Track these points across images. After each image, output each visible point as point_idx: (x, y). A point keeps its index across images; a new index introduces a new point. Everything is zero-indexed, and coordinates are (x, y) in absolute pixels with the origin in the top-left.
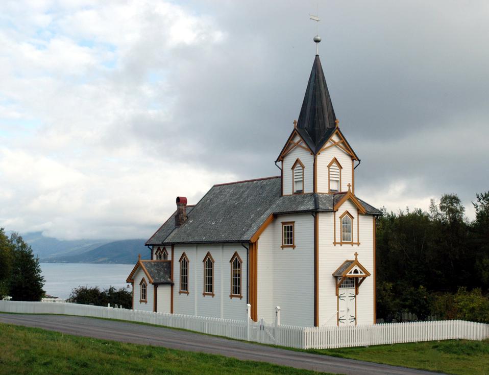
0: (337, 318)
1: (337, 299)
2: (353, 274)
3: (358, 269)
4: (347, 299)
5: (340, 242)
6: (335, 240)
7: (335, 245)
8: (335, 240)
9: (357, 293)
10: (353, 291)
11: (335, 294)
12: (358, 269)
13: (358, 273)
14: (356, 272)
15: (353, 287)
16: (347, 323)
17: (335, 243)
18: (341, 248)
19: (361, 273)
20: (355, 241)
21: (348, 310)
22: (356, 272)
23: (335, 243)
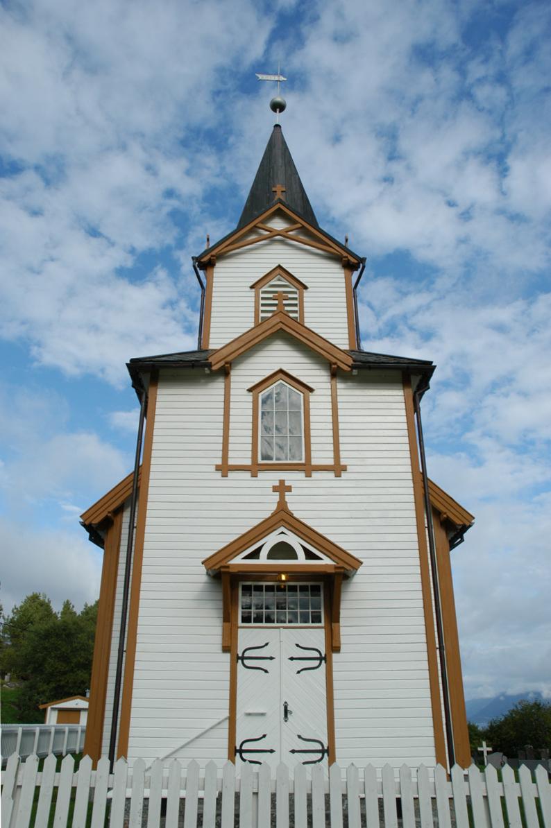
0: (226, 743)
1: (227, 667)
2: (263, 560)
3: (294, 541)
4: (282, 669)
5: (248, 462)
6: (225, 456)
7: (225, 475)
8: (225, 456)
9: (333, 646)
10: (315, 637)
11: (219, 648)
12: (294, 541)
13: (295, 556)
14: (283, 550)
15: (316, 619)
16: (284, 769)
17: (225, 469)
18: (254, 482)
19: (309, 555)
20: (322, 455)
21: (286, 712)
22: (283, 550)
23: (225, 469)
